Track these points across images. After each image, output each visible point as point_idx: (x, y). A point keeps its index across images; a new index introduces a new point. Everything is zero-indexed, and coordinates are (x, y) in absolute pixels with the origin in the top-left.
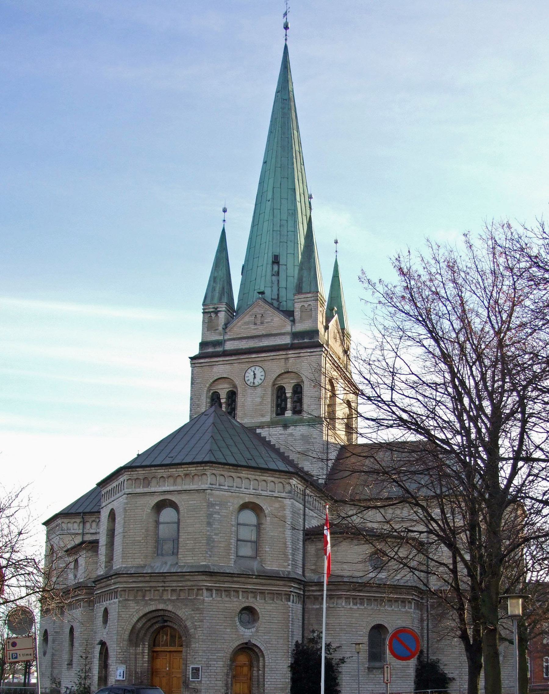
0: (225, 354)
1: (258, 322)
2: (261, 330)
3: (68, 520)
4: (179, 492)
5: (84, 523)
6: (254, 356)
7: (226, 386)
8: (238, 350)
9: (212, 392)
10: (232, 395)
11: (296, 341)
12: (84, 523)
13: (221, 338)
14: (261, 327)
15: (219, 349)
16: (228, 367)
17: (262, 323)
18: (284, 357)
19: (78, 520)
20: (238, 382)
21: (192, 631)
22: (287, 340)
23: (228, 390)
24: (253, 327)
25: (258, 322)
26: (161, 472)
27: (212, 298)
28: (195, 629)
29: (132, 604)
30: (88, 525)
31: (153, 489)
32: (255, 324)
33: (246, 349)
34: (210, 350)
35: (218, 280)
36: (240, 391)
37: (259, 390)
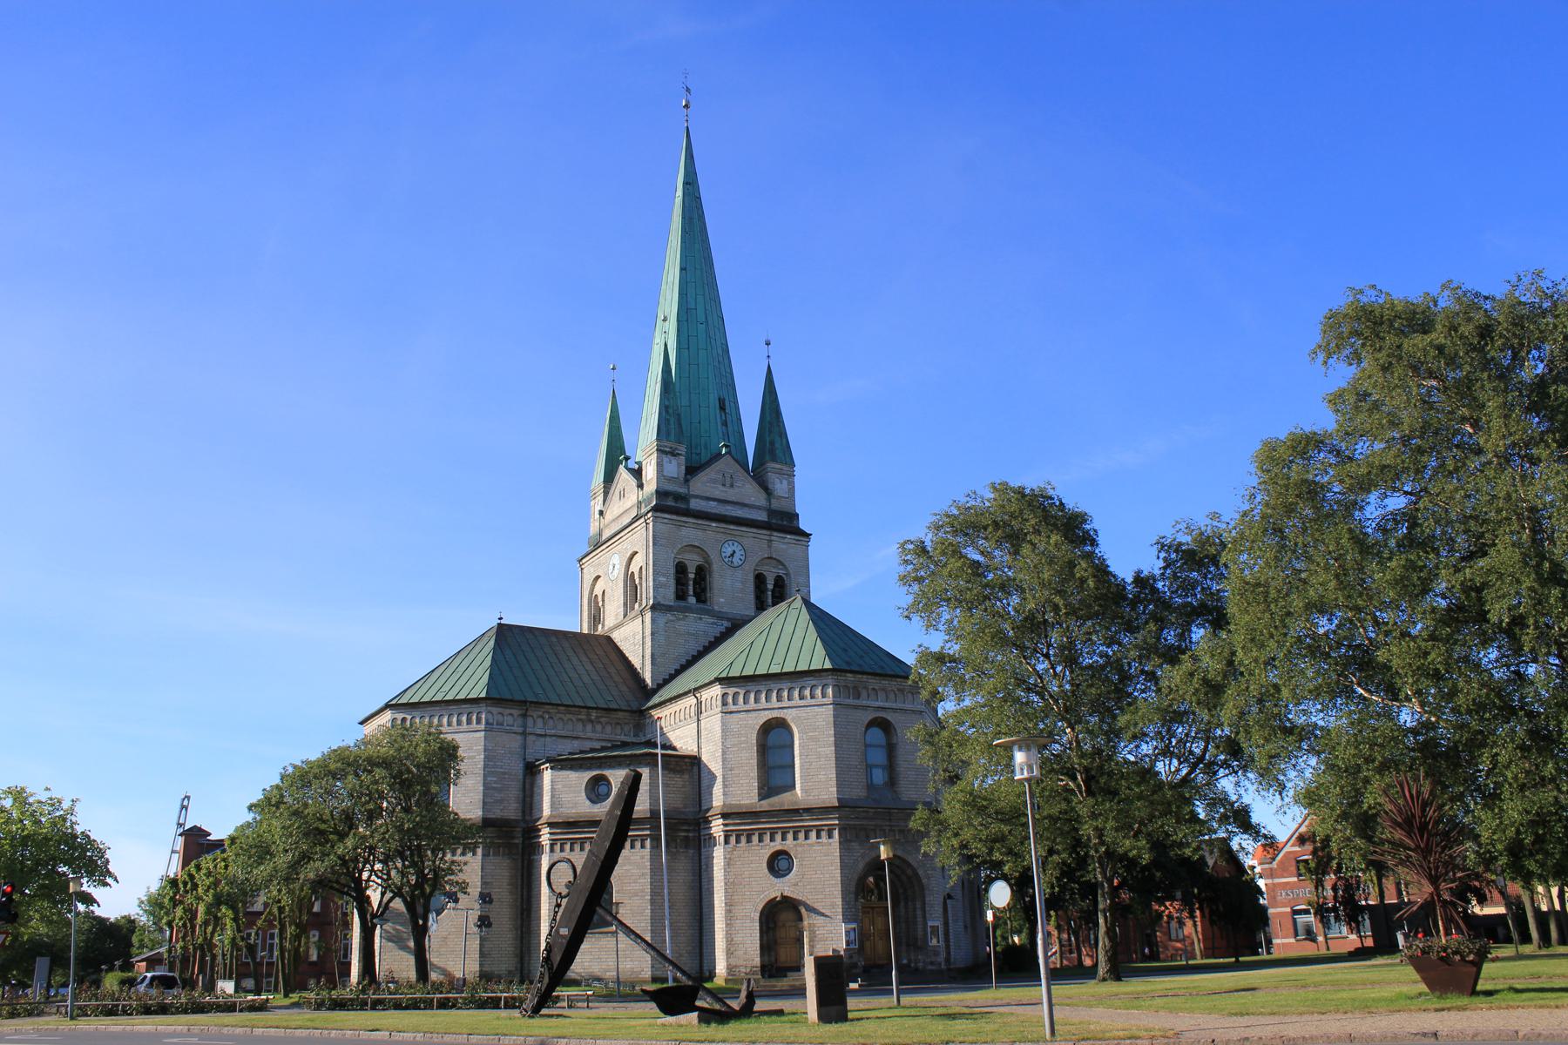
0: (688, 513)
1: (728, 484)
2: (731, 494)
3: (500, 710)
4: (894, 710)
5: (524, 716)
6: (732, 527)
7: (695, 557)
8: (725, 516)
9: (677, 560)
10: (702, 573)
11: (774, 521)
12: (524, 716)
13: (682, 490)
14: (731, 491)
15: (682, 506)
16: (700, 533)
17: (732, 486)
18: (767, 538)
19: (516, 712)
20: (714, 557)
21: (924, 881)
22: (762, 516)
23: (698, 563)
24: (721, 488)
25: (728, 484)
26: (873, 682)
27: (668, 434)
28: (929, 878)
29: (855, 845)
30: (530, 721)
31: (864, 703)
32: (724, 485)
33: (716, 514)
34: (670, 502)
35: (671, 411)
36: (715, 567)
37: (739, 574)
